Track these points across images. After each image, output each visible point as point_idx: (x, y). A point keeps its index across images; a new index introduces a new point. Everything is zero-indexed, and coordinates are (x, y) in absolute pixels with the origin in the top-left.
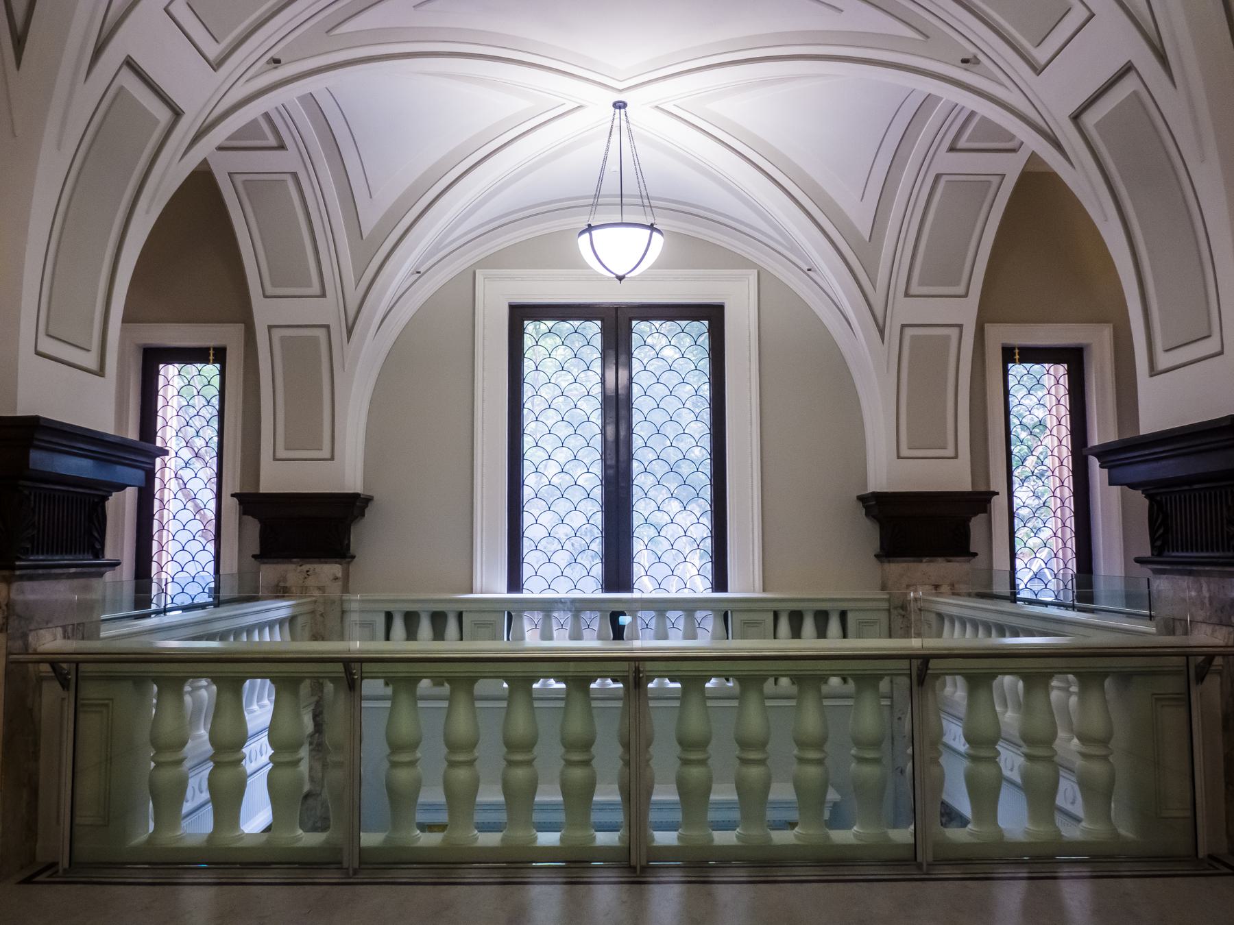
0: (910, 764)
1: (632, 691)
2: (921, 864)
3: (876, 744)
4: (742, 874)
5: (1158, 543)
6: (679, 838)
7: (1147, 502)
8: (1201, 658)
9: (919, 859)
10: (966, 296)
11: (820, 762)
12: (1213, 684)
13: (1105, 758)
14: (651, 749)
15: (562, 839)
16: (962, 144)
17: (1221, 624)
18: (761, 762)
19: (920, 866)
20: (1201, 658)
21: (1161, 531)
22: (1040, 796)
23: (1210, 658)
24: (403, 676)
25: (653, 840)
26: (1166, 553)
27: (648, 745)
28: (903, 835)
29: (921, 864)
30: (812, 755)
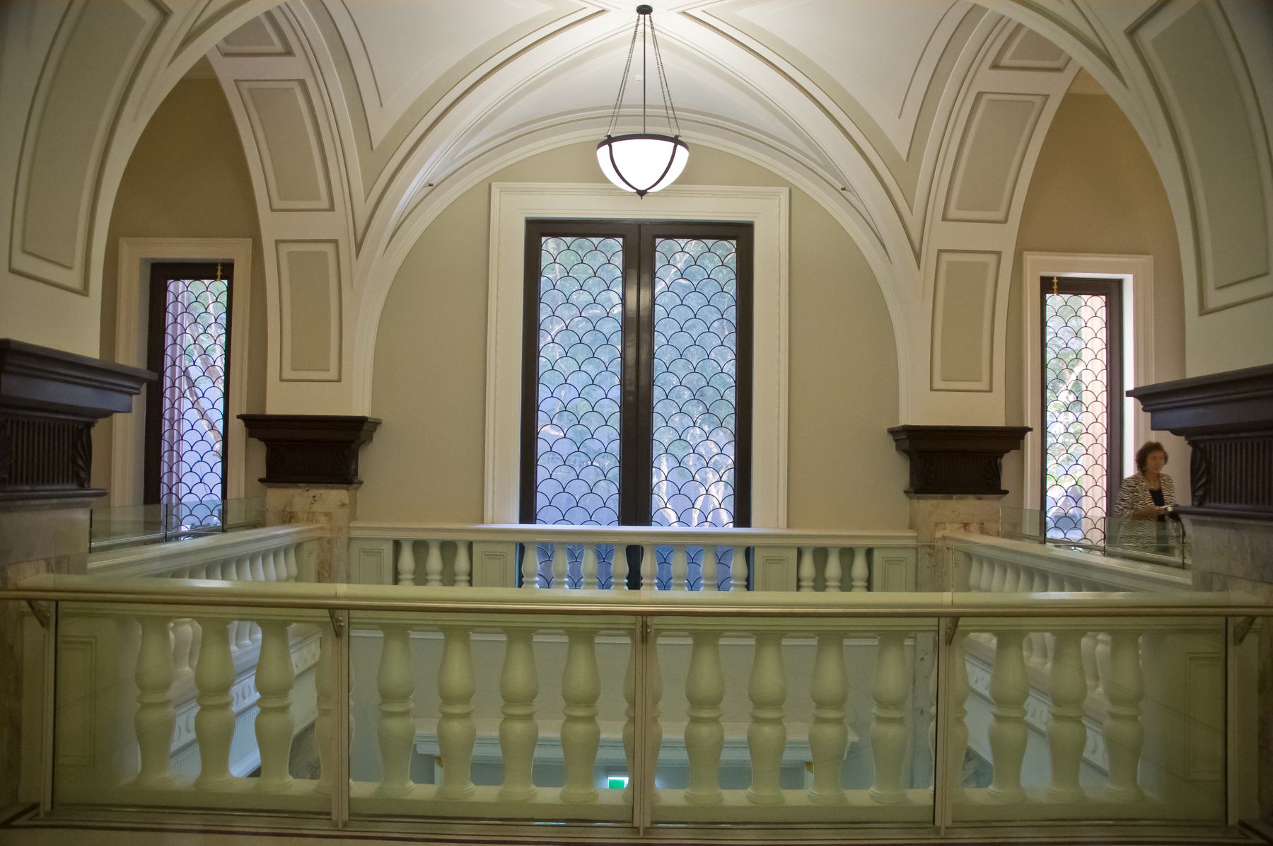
0: (933, 724)
3: (898, 704)
5: (1200, 493)
7: (1190, 449)
8: (1240, 619)
9: (937, 823)
10: (1005, 221)
11: (838, 721)
12: (1252, 640)
13: (1134, 718)
14: (661, 704)
16: (1005, 61)
17: (1262, 580)
18: (778, 721)
19: (937, 831)
20: (1240, 619)
21: (1203, 480)
22: (1067, 758)
23: (1252, 619)
24: (396, 622)
26: (1207, 504)
27: (655, 703)
28: (921, 796)
30: (831, 714)
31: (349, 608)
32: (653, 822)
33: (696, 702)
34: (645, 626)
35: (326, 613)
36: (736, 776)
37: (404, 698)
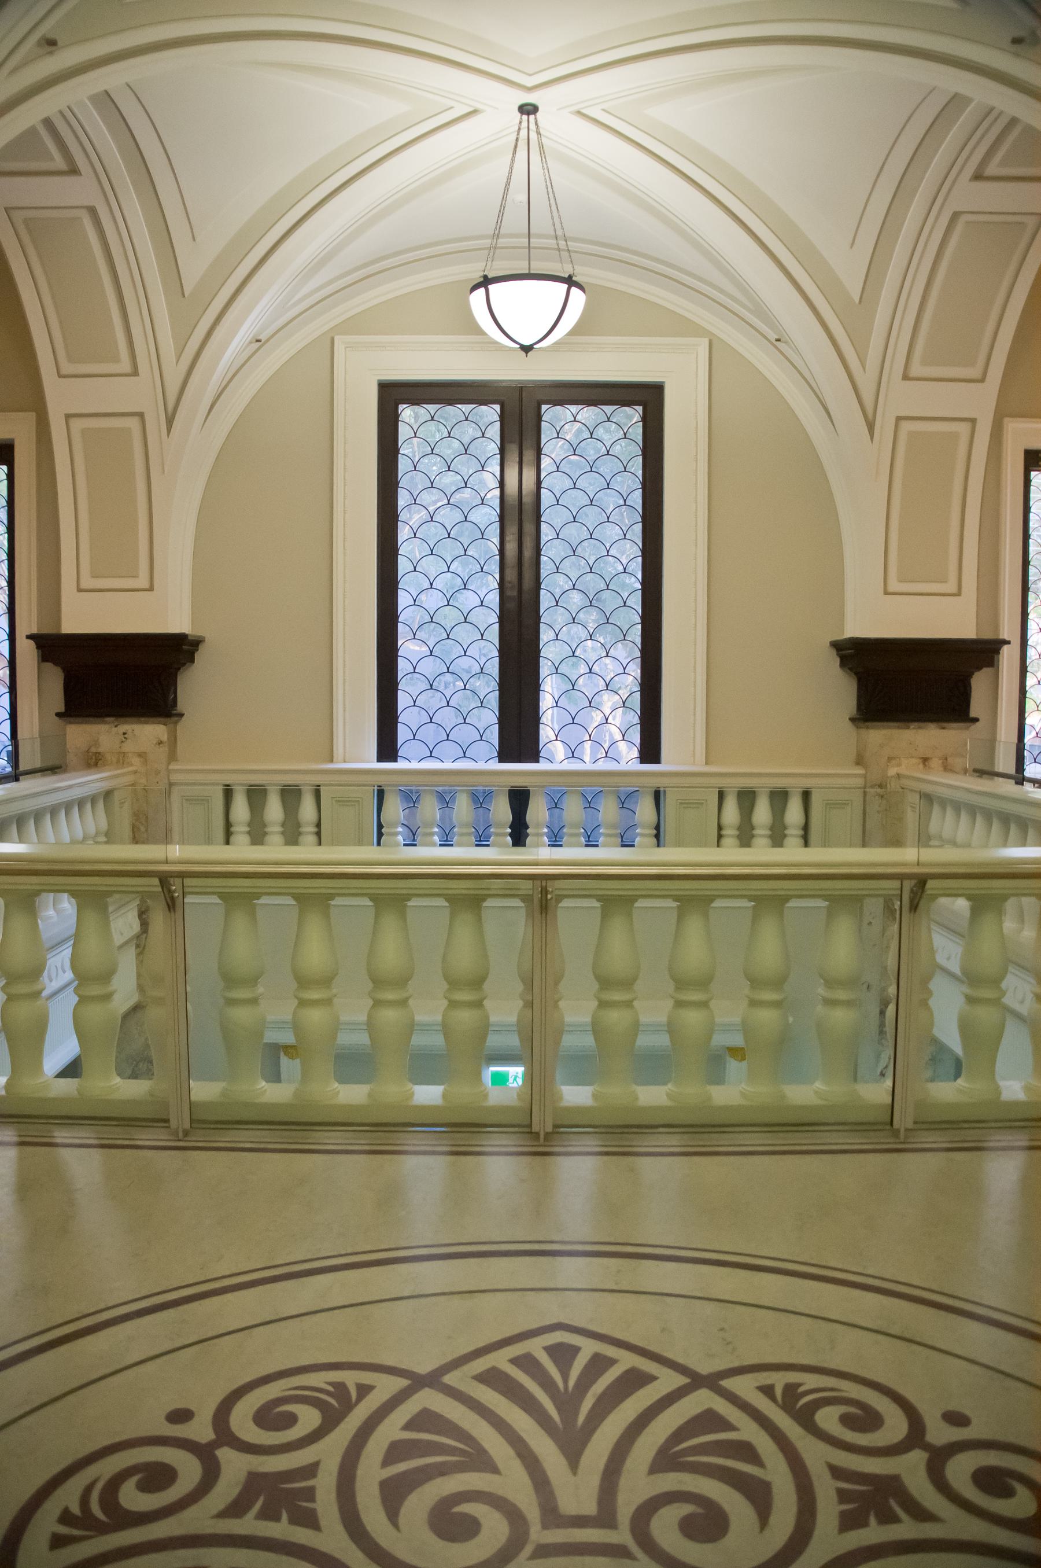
1: (537, 915)
4: (673, 1141)
6: (595, 1096)
14: (562, 986)
15: (444, 1096)
18: (704, 1005)
24: (239, 891)
25: (561, 1098)
27: (557, 983)
31: (182, 875)
32: (555, 1126)
33: (605, 982)
34: (544, 891)
35: (156, 881)
36: (654, 1066)
37: (252, 981)
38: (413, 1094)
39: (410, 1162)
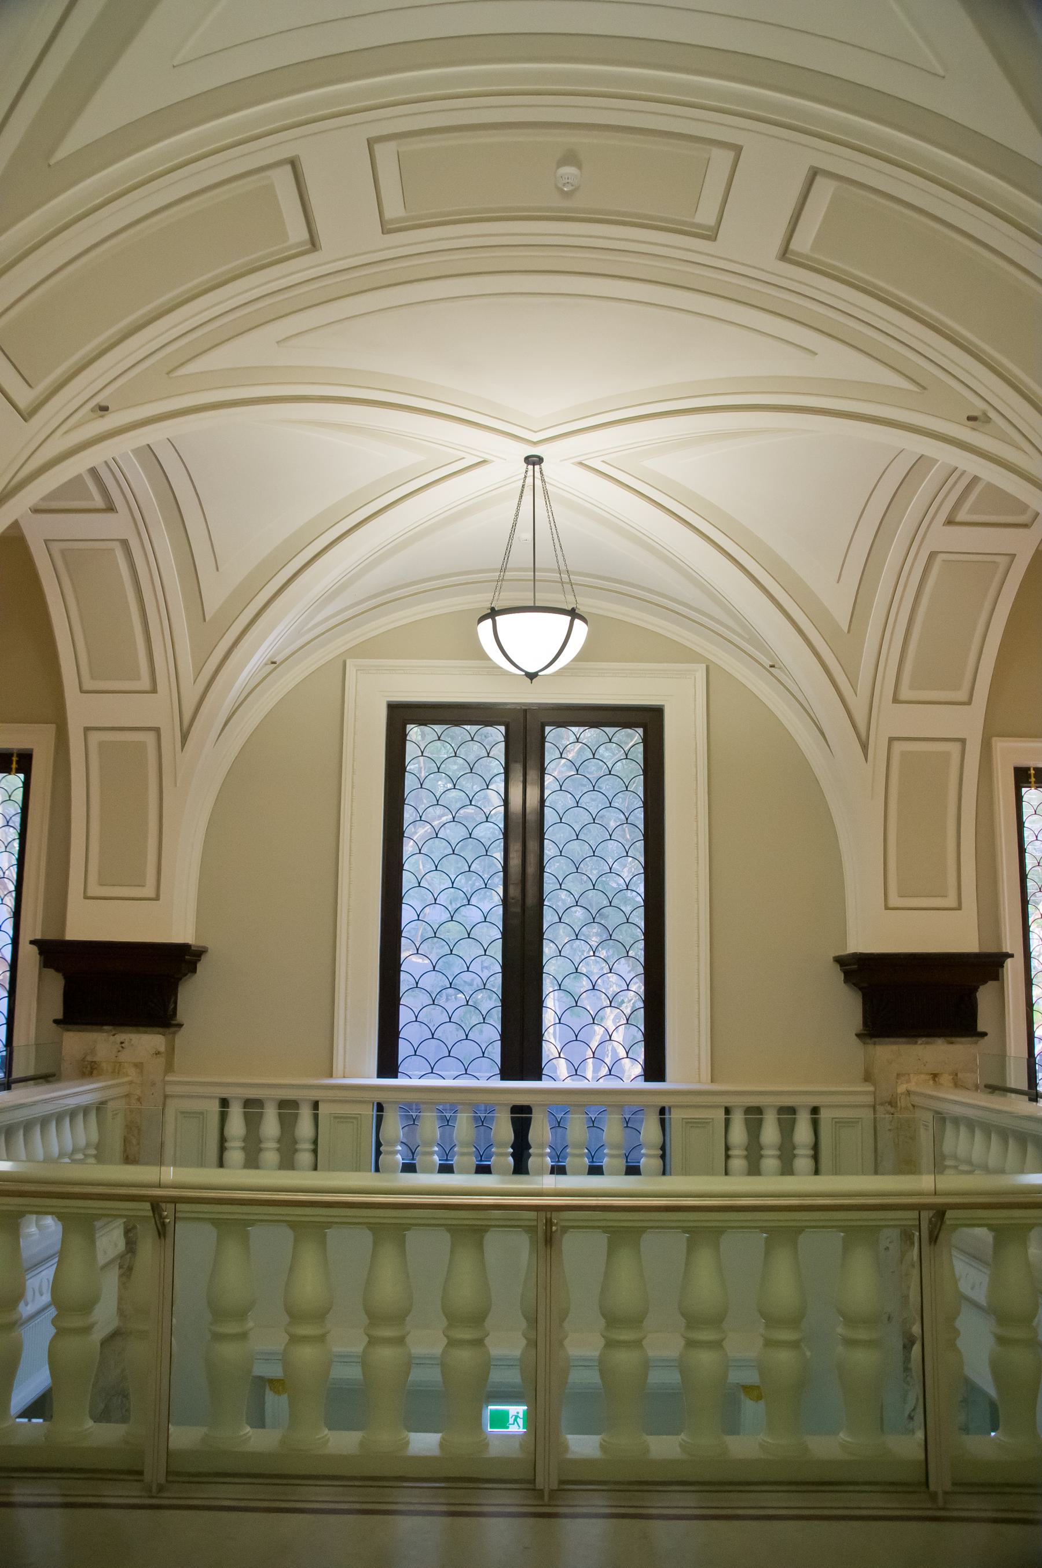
2: (936, 1493)
4: (688, 1501)
6: (603, 1447)
11: (795, 1345)
14: (566, 1324)
15: (442, 1445)
25: (566, 1449)
27: (562, 1320)
29: (936, 1493)
32: (562, 1482)
33: (612, 1320)
38: (407, 1443)
39: (405, 1524)
